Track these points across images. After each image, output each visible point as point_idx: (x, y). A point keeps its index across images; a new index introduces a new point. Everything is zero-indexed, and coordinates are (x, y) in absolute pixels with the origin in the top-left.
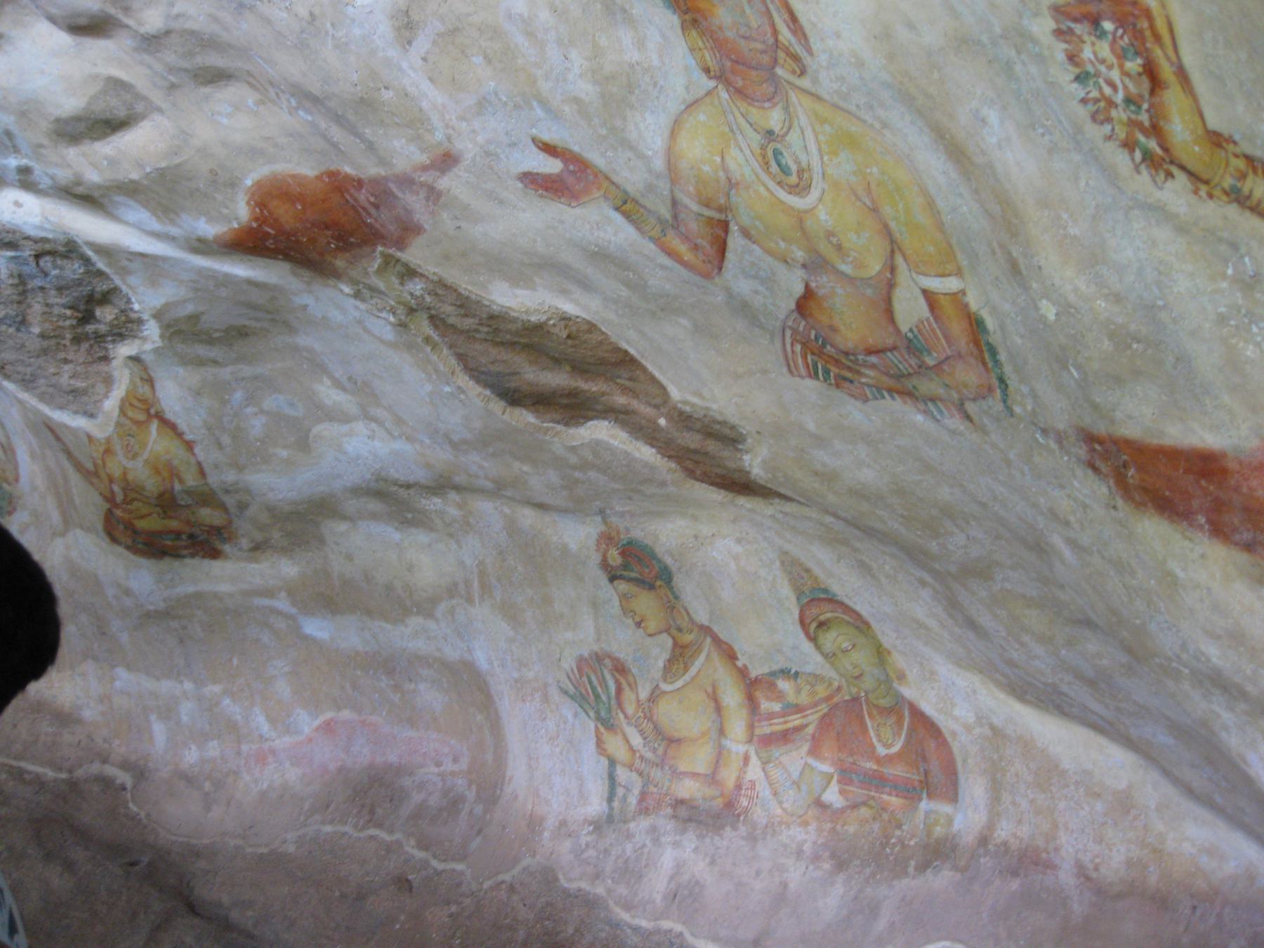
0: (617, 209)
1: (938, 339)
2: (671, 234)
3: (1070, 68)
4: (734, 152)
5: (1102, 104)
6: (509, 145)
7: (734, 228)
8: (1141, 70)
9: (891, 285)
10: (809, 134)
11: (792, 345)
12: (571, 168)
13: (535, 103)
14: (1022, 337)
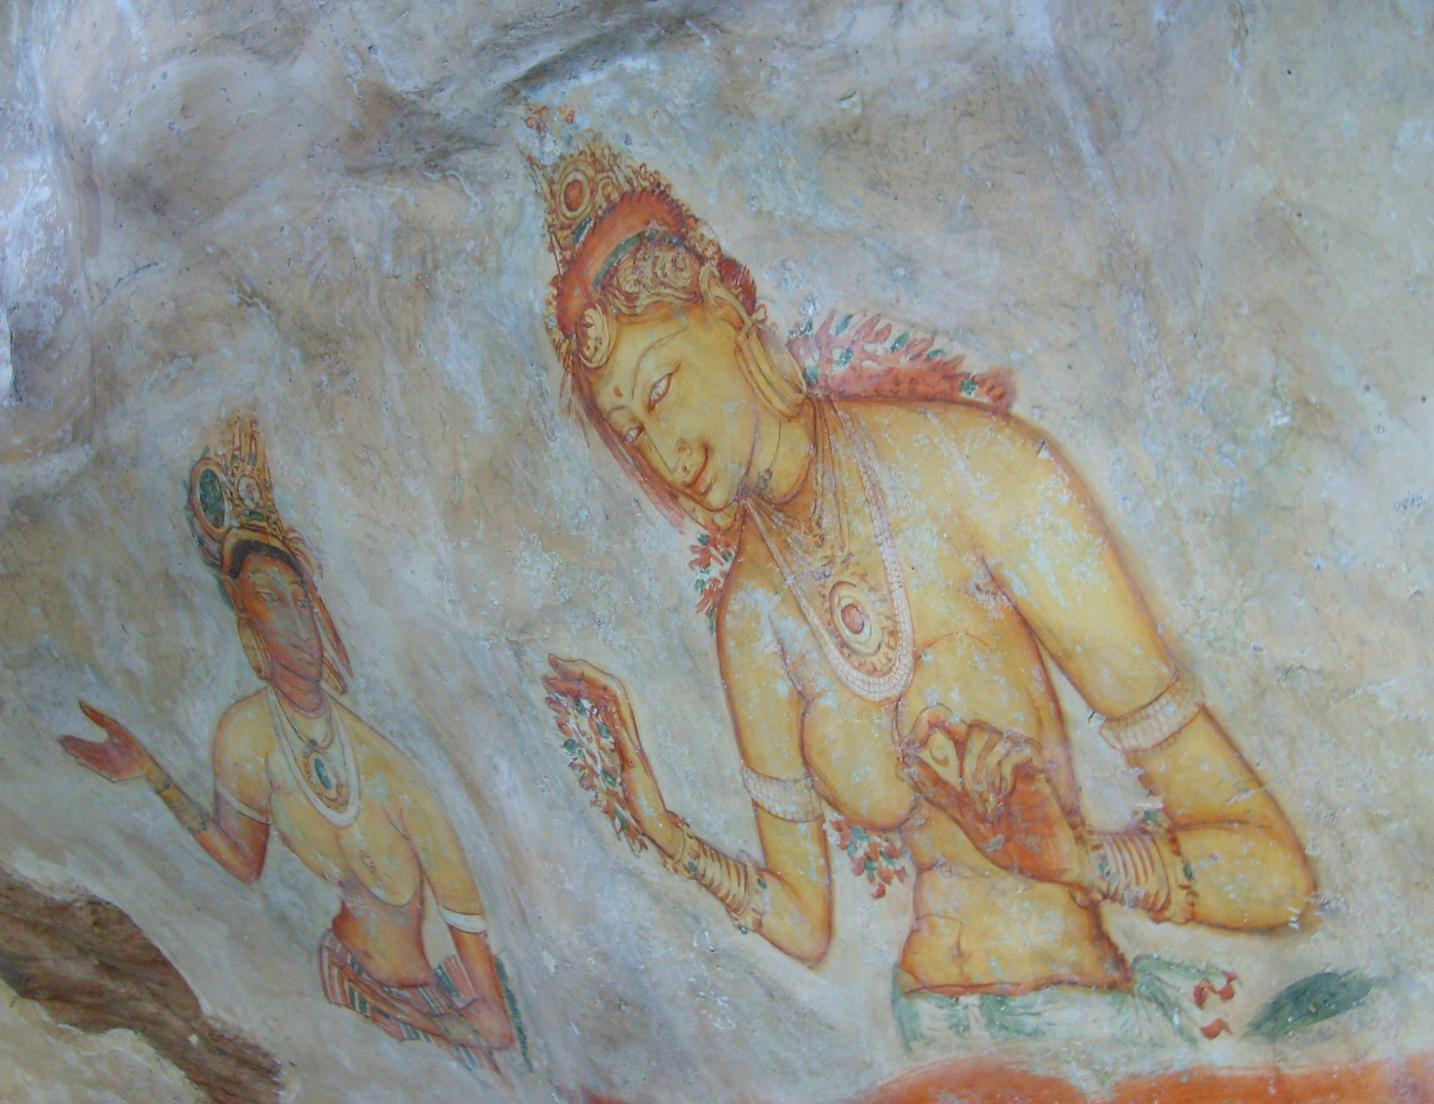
0: (158, 792)
2: (211, 828)
3: (560, 734)
4: (277, 756)
5: (587, 771)
6: (54, 704)
7: (274, 833)
8: (613, 747)
9: (420, 917)
10: (348, 751)
11: (329, 968)
12: (116, 740)
13: (86, 666)
14: (536, 987)
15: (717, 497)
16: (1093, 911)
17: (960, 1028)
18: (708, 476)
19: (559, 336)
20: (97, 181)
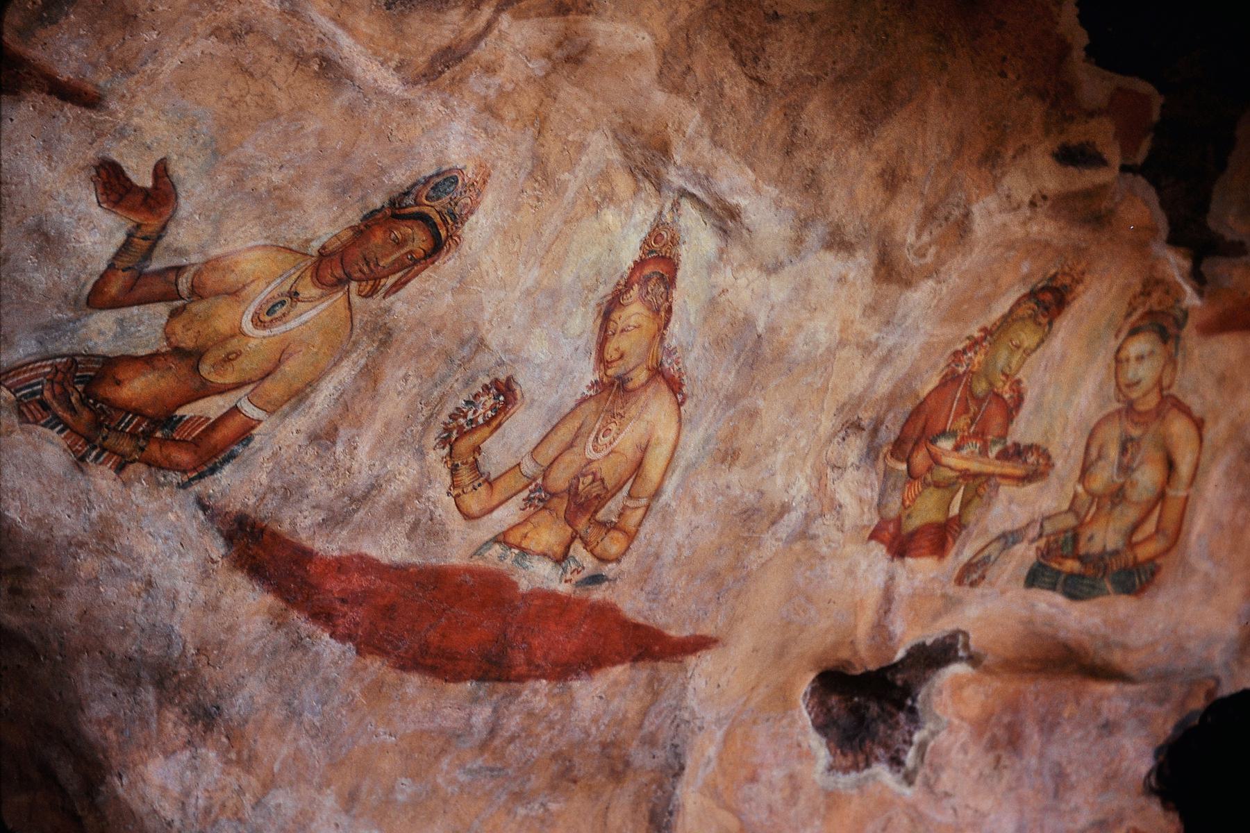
1: (194, 429)
10: (313, 313)
15: (610, 372)
16: (573, 539)
17: (502, 558)
18: (615, 364)
19: (622, 282)
20: (570, 17)
